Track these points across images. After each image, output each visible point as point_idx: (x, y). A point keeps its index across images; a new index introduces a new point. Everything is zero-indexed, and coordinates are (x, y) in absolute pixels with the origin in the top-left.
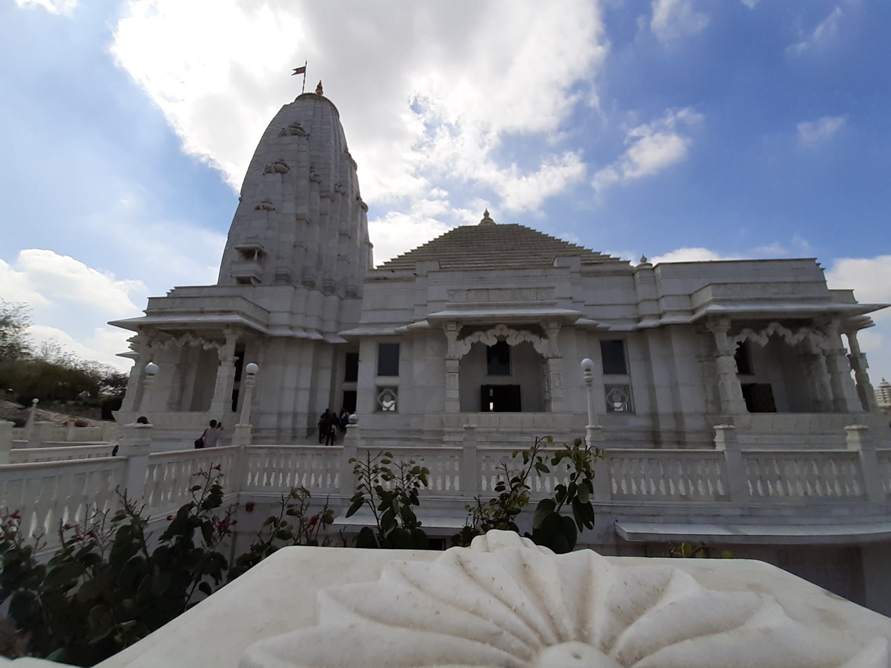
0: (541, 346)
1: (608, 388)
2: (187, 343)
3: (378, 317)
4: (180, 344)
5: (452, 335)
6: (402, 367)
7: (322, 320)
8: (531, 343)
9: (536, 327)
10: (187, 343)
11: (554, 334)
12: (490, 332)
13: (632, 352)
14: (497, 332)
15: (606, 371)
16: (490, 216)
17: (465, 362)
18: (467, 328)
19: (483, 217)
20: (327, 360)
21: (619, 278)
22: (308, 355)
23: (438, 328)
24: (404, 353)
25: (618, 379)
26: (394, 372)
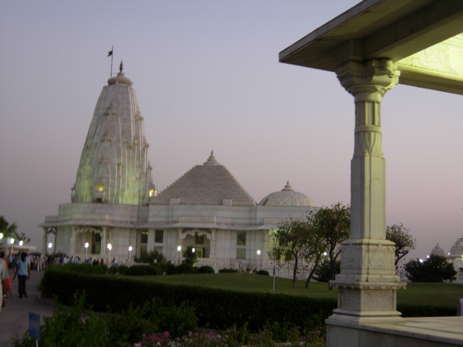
0: (209, 236)
1: (238, 249)
2: (89, 231)
3: (155, 219)
4: (87, 230)
5: (180, 232)
6: (164, 239)
7: (132, 217)
8: (206, 236)
9: (208, 230)
10: (89, 231)
11: (213, 233)
12: (193, 231)
13: (247, 237)
14: (195, 231)
15: (238, 244)
16: (214, 155)
17: (185, 240)
18: (185, 230)
19: (210, 155)
20: (134, 234)
21: (247, 208)
22: (127, 233)
23: (176, 229)
24: (165, 234)
25: (242, 247)
26: (162, 242)
